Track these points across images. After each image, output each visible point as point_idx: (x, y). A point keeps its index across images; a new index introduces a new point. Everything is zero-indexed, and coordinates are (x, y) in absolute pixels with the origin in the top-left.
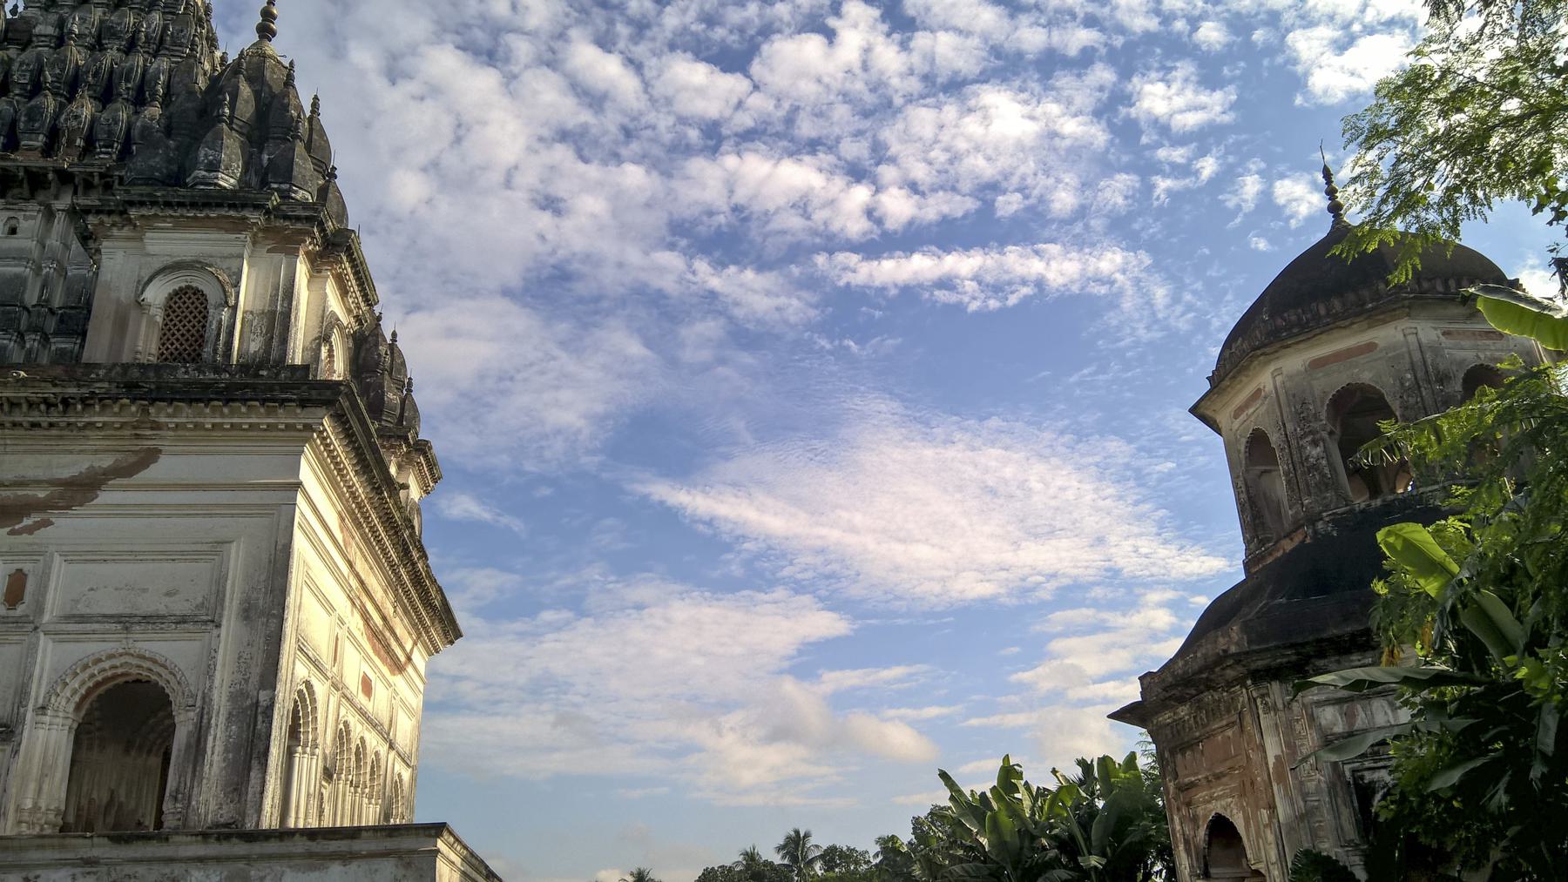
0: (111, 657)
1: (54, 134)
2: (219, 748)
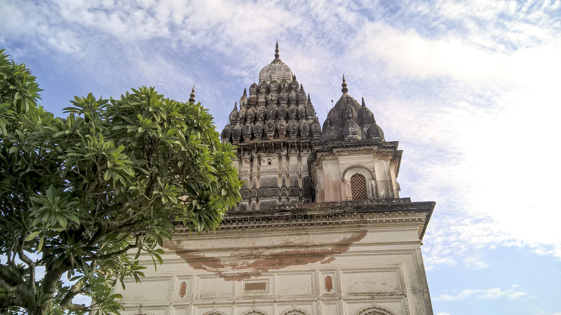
0: (369, 309)
1: (277, 131)
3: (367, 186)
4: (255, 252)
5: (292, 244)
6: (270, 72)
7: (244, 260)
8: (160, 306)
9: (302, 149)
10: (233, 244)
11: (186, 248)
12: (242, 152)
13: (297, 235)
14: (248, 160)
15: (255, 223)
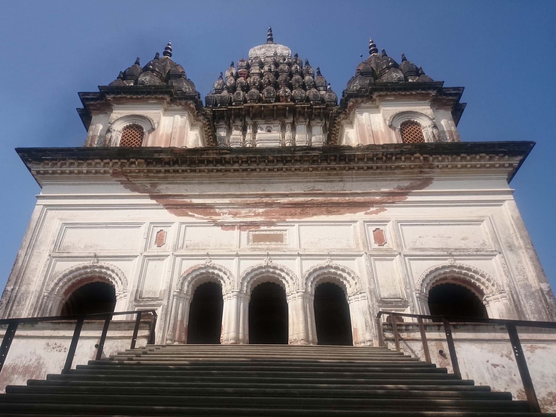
2: (529, 312)
3: (424, 134)
11: (164, 193)
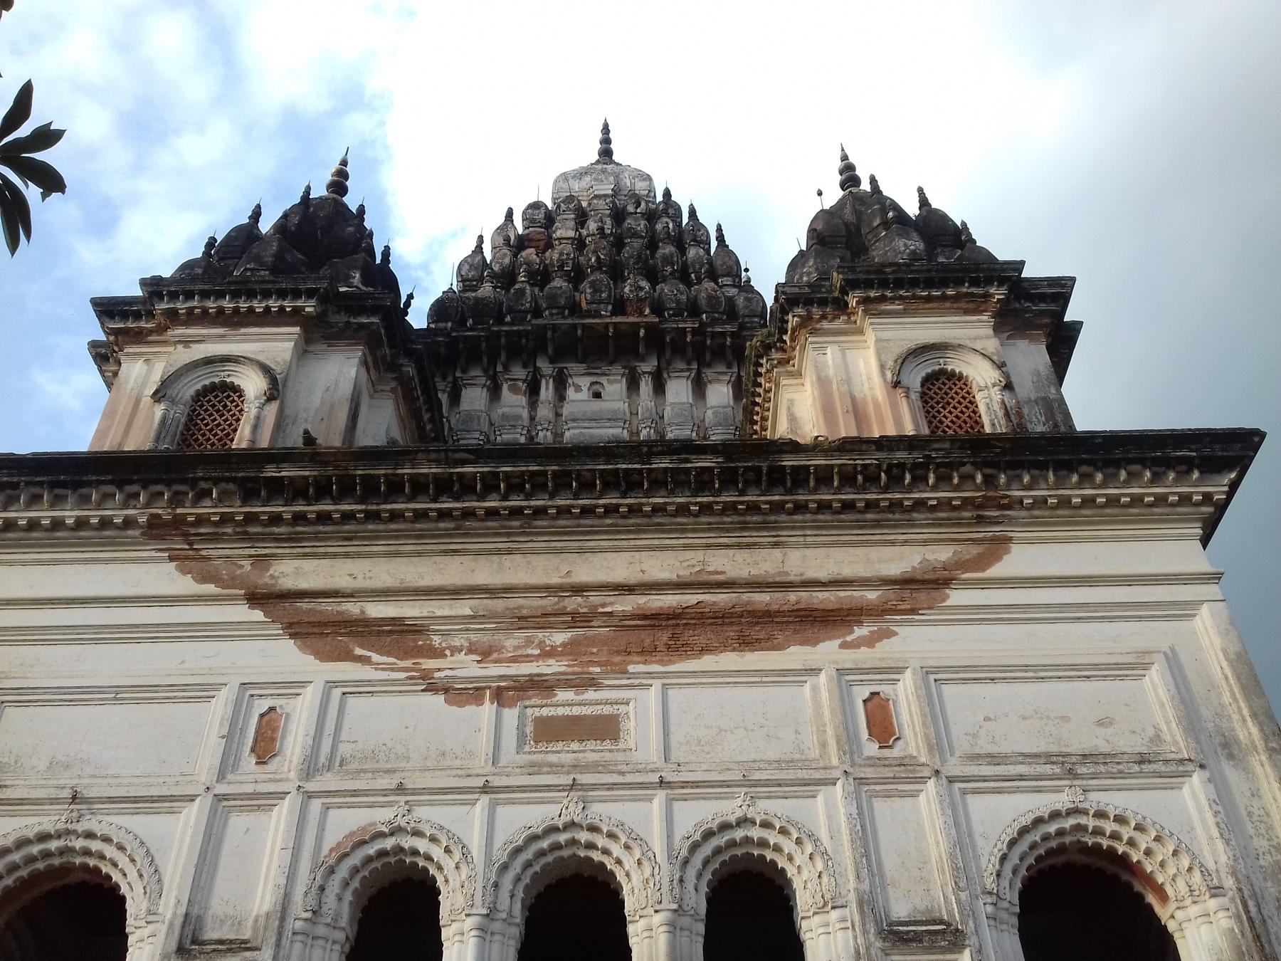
0: (1055, 815)
3: (982, 409)
4: (573, 603)
5: (721, 578)
6: (588, 178)
7: (529, 633)
8: (162, 799)
9: (708, 356)
10: (484, 572)
11: (288, 583)
12: (503, 357)
13: (739, 546)
14: (524, 387)
15: (576, 497)
